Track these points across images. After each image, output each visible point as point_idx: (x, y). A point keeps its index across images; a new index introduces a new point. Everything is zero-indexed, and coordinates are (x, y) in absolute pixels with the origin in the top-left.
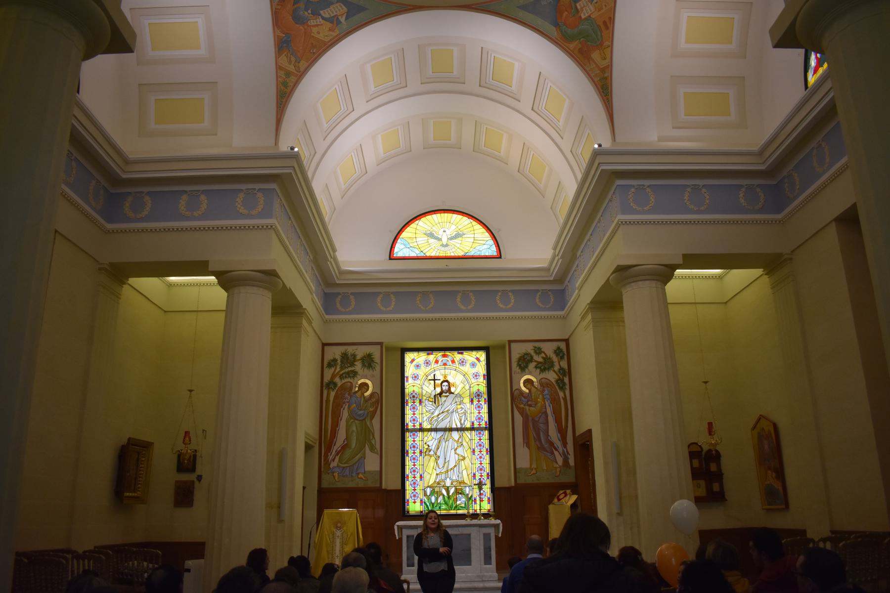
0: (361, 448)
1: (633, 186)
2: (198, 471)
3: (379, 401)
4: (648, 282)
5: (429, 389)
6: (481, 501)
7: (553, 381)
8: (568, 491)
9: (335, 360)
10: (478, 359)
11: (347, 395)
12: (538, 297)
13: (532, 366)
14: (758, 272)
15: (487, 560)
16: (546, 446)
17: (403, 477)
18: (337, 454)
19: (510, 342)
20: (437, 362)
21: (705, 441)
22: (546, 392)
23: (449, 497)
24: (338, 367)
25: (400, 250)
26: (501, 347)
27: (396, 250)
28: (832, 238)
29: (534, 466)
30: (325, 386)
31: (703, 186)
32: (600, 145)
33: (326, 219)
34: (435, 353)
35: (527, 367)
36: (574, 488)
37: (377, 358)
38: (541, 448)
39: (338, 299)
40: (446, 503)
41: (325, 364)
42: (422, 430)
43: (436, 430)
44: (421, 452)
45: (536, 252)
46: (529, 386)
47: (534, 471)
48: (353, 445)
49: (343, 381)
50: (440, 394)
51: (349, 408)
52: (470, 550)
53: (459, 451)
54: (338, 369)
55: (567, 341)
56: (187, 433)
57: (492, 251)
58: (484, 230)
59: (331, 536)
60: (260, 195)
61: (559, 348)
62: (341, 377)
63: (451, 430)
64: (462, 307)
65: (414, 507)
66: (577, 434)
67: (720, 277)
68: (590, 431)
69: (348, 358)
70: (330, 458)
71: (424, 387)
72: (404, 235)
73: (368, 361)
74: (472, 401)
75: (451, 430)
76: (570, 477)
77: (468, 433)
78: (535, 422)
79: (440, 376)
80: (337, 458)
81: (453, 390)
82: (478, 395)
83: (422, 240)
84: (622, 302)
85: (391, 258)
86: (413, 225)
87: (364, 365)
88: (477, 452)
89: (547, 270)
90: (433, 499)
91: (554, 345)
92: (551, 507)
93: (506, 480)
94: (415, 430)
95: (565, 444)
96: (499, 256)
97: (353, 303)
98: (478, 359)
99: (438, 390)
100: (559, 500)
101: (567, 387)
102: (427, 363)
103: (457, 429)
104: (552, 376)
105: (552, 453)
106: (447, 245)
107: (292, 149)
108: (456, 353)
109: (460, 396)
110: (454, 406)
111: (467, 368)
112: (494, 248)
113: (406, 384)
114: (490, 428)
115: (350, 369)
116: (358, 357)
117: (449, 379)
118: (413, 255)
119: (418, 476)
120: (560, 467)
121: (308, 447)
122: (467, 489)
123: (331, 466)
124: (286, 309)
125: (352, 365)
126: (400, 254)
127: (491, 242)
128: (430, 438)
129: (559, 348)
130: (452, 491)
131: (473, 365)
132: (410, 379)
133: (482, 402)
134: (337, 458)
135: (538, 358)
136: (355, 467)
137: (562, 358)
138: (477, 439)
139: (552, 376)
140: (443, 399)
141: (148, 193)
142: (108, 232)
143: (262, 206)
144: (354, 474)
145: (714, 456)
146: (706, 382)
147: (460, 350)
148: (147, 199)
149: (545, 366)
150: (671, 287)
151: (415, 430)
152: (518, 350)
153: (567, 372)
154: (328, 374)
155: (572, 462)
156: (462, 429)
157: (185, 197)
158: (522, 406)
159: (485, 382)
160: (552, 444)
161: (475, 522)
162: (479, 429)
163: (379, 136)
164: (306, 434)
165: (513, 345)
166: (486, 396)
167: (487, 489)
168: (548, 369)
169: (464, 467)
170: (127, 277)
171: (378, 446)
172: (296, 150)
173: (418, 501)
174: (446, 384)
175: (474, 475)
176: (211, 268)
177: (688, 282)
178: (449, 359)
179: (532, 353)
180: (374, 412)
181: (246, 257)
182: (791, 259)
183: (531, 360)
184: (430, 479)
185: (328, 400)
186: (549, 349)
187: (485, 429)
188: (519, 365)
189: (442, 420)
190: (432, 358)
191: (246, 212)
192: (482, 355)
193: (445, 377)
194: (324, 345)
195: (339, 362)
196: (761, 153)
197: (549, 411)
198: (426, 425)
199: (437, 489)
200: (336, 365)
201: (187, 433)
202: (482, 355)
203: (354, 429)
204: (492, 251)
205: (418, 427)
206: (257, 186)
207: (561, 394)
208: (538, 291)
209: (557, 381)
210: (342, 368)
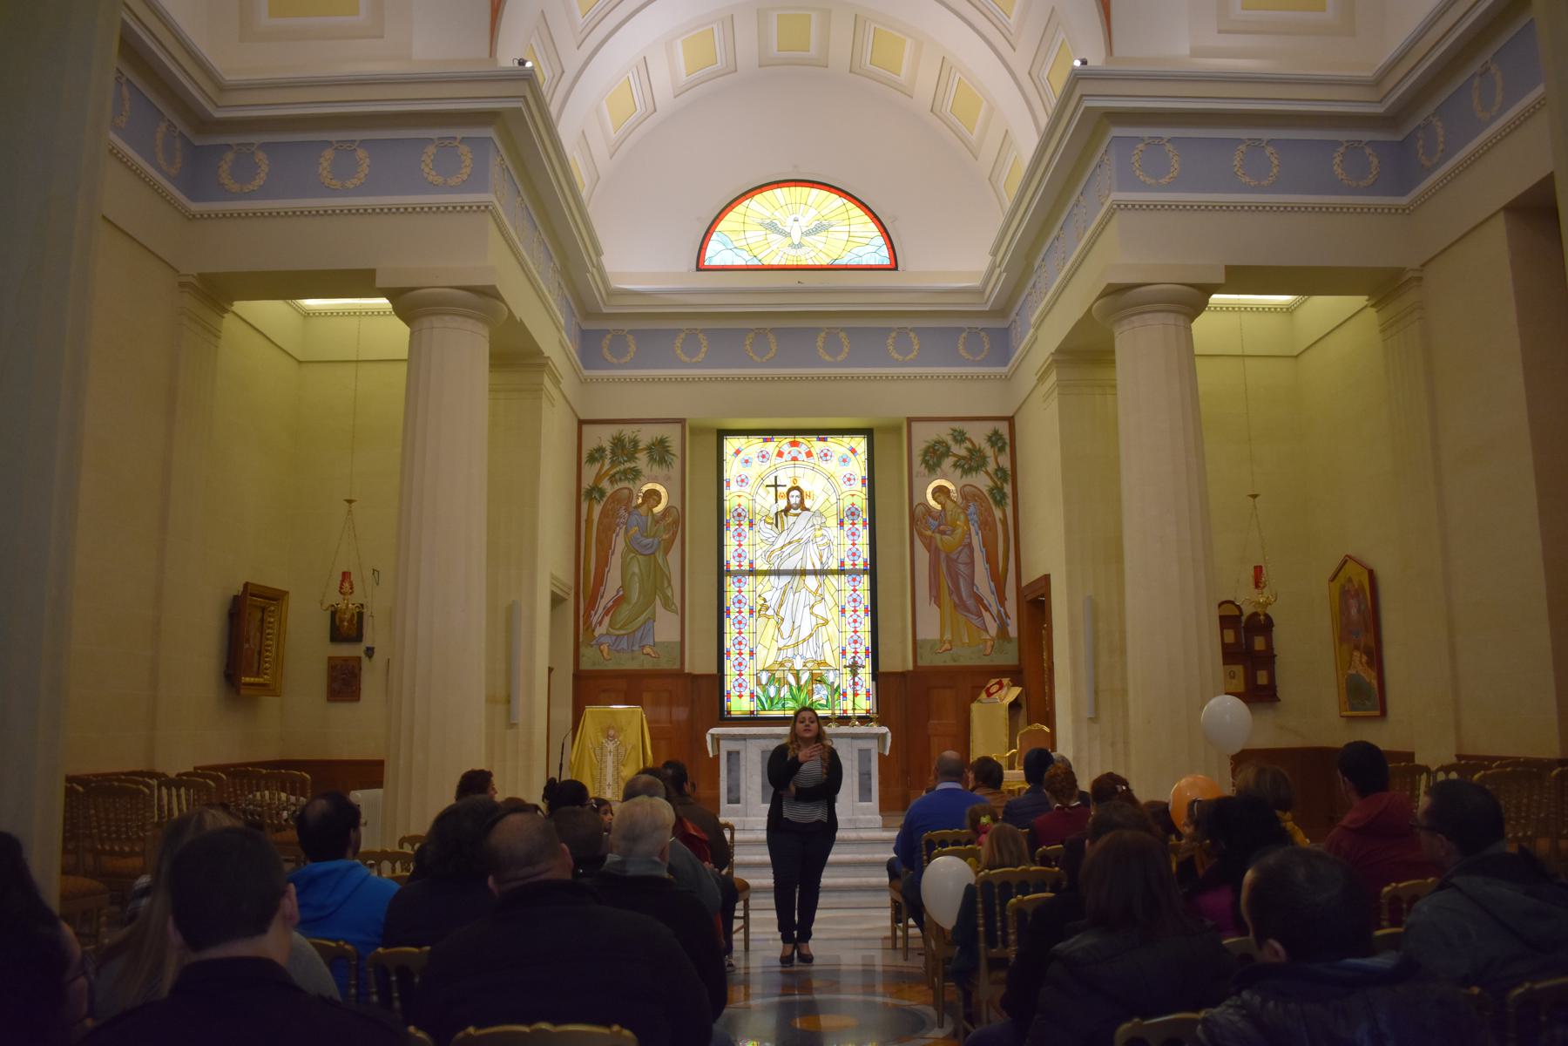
0: (650, 603)
1: (1142, 139)
2: (368, 641)
3: (680, 521)
4: (1160, 315)
5: (767, 503)
6: (855, 695)
7: (985, 490)
8: (1006, 681)
9: (601, 450)
10: (853, 451)
11: (622, 512)
12: (961, 341)
13: (948, 463)
14: (1360, 301)
15: (865, 794)
16: (970, 603)
17: (721, 654)
18: (606, 614)
19: (910, 420)
20: (780, 454)
21: (1248, 600)
22: (972, 509)
23: (799, 688)
24: (607, 462)
25: (716, 254)
26: (894, 430)
27: (709, 253)
28: (1496, 243)
29: (948, 636)
30: (584, 495)
31: (1270, 142)
32: (1084, 62)
33: (584, 194)
34: (777, 439)
35: (938, 464)
36: (1015, 675)
37: (675, 446)
38: (960, 606)
39: (606, 342)
40: (794, 698)
41: (583, 457)
42: (753, 572)
43: (778, 573)
44: (751, 612)
45: (959, 259)
46: (942, 498)
47: (947, 646)
48: (635, 596)
49: (616, 487)
50: (786, 511)
51: (627, 531)
53: (817, 610)
54: (606, 467)
55: (1011, 420)
56: (346, 575)
57: (882, 257)
58: (867, 219)
59: (598, 751)
60: (464, 149)
61: (996, 433)
62: (613, 480)
63: (804, 573)
64: (827, 358)
65: (739, 705)
66: (1024, 583)
67: (1289, 310)
68: (1047, 578)
69: (623, 447)
70: (595, 620)
71: (758, 499)
72: (721, 226)
73: (659, 452)
74: (841, 523)
75: (804, 573)
76: (1009, 657)
77: (833, 579)
78: (951, 562)
79: (785, 480)
80: (607, 620)
81: (807, 503)
82: (853, 513)
83: (756, 235)
84: (1113, 352)
85: (700, 267)
86: (740, 209)
87: (652, 459)
88: (849, 612)
89: (979, 292)
91: (988, 427)
92: (975, 707)
93: (899, 659)
94: (740, 573)
95: (1002, 600)
96: (894, 267)
97: (633, 348)
98: (853, 451)
99: (783, 504)
100: (989, 695)
101: (1009, 501)
103: (815, 573)
104: (982, 481)
105: (980, 615)
106: (800, 245)
107: (522, 63)
108: (814, 438)
109: (821, 515)
110: (809, 533)
111: (833, 466)
112: (885, 251)
113: (726, 492)
114: (872, 571)
115: (628, 465)
116: (642, 445)
118: (739, 262)
119: (746, 651)
120: (993, 639)
121: (556, 601)
123: (596, 634)
124: (515, 357)
125: (632, 458)
126: (716, 262)
127: (881, 241)
128: (768, 587)
129: (996, 433)
130: (805, 677)
132: (733, 483)
133: (859, 526)
134: (607, 620)
135: (960, 450)
136: (638, 635)
137: (1001, 449)
138: (849, 591)
139: (982, 481)
140: (791, 519)
141: (265, 146)
142: (193, 217)
143: (468, 170)
145: (1261, 625)
146: (1254, 496)
147: (822, 433)
148: (261, 156)
149: (972, 462)
150: (1202, 326)
151: (740, 573)
152: (925, 435)
153: (1009, 475)
154: (590, 473)
155: (1013, 631)
156: (822, 573)
157: (328, 154)
158: (929, 533)
159: (865, 490)
160: (979, 600)
161: (844, 729)
162: (854, 572)
163: (679, 42)
164: (553, 577)
165: (915, 425)
166: (865, 516)
167: (865, 675)
168: (977, 469)
170: (231, 300)
171: (677, 601)
172: (529, 64)
173: (746, 693)
174: (796, 493)
176: (380, 283)
177: (1235, 317)
178: (803, 449)
179: (950, 442)
181: (445, 264)
182: (1420, 279)
183: (947, 452)
184: (767, 656)
185: (589, 521)
186: (978, 434)
187: (864, 572)
188: (925, 462)
189: (789, 555)
190: (771, 447)
191: (439, 180)
192: (860, 443)
193: (795, 480)
194: (581, 423)
196: (1377, 82)
197: (976, 541)
198: (761, 565)
200: (602, 458)
201: (346, 575)
202: (860, 443)
203: (636, 570)
204: (882, 257)
205: (746, 567)
206: (460, 133)
207: (998, 514)
208: (961, 330)
209: (991, 491)
210: (612, 462)
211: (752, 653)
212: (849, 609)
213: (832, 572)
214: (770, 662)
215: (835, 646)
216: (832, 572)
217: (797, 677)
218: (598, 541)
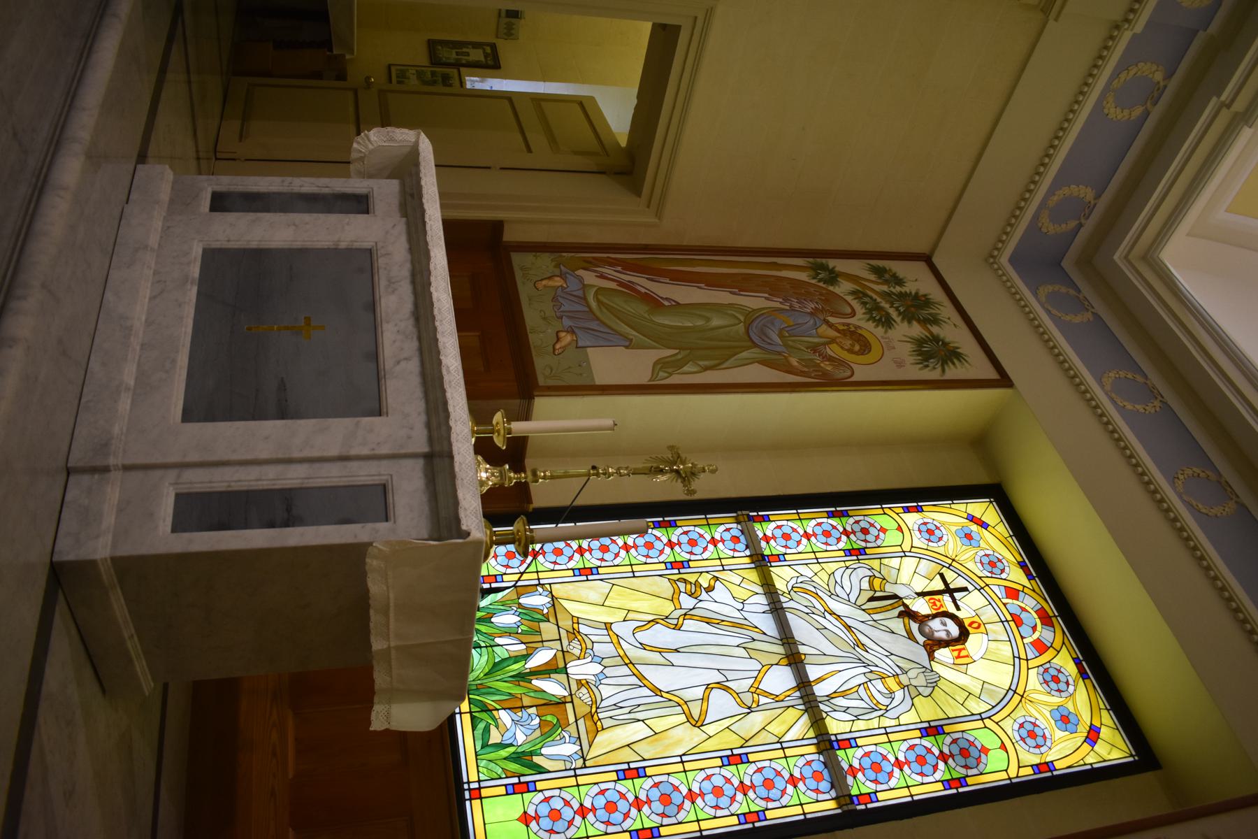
0: (659, 338)
5: (911, 578)
18: (621, 284)
20: (1012, 593)
23: (522, 677)
24: (885, 288)
40: (496, 667)
42: (761, 562)
43: (776, 609)
49: (849, 298)
52: (282, 414)
53: (721, 703)
63: (795, 660)
70: (607, 271)
75: (795, 660)
77: (800, 727)
79: (970, 606)
80: (613, 285)
81: (943, 654)
82: (968, 753)
90: (507, 619)
102: (993, 564)
103: (804, 684)
109: (933, 685)
111: (1041, 705)
116: (935, 329)
117: (975, 643)
122: (569, 749)
123: (580, 272)
125: (908, 317)
128: (741, 593)
130: (552, 687)
131: (1065, 720)
133: (942, 773)
134: (613, 285)
136: (594, 325)
140: (898, 625)
144: (567, 322)
162: (837, 777)
169: (659, 725)
171: (676, 379)
175: (639, 773)
180: (790, 370)
184: (584, 602)
187: (843, 797)
190: (1017, 576)
195: (898, 289)
199: (548, 629)
211: (586, 572)
212: (745, 772)
213: (817, 721)
214: (574, 608)
215: (646, 750)
216: (817, 721)
217: (546, 671)
218: (747, 277)
